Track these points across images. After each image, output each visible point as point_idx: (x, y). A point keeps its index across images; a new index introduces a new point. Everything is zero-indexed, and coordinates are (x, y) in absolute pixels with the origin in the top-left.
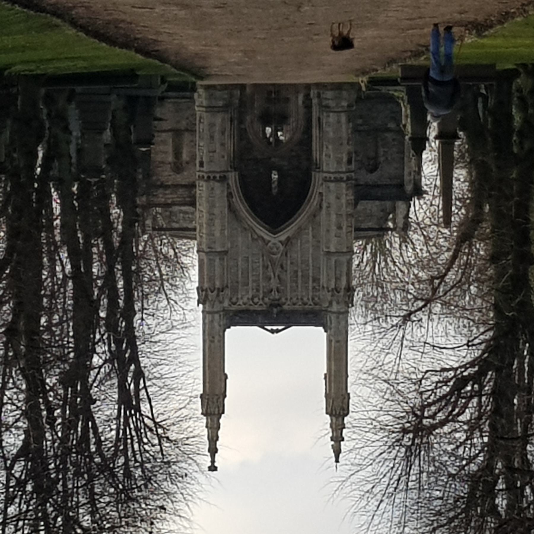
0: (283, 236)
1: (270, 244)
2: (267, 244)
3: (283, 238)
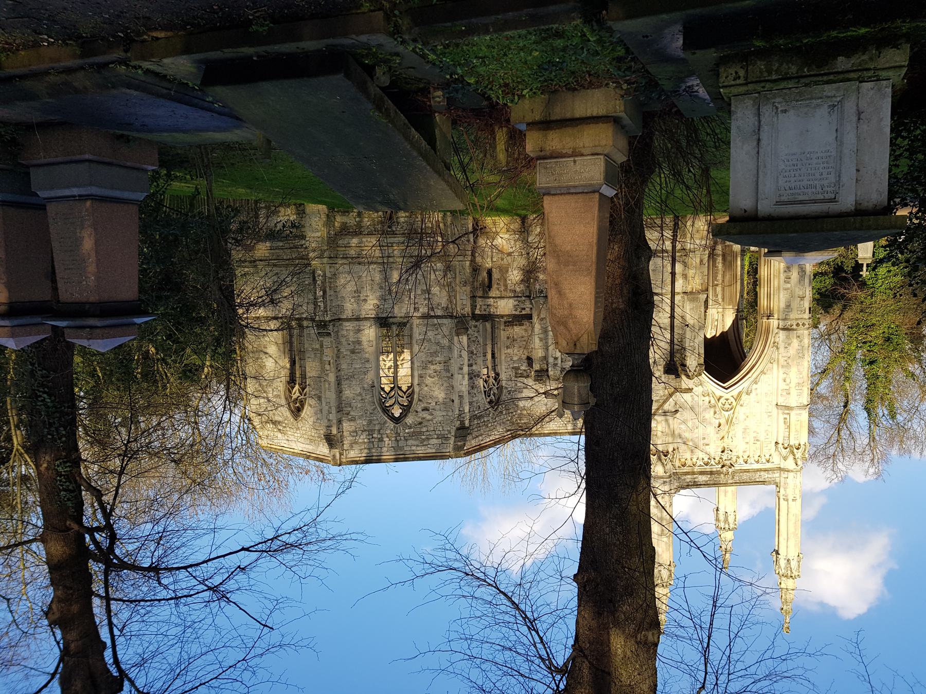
0: (735, 391)
1: (722, 400)
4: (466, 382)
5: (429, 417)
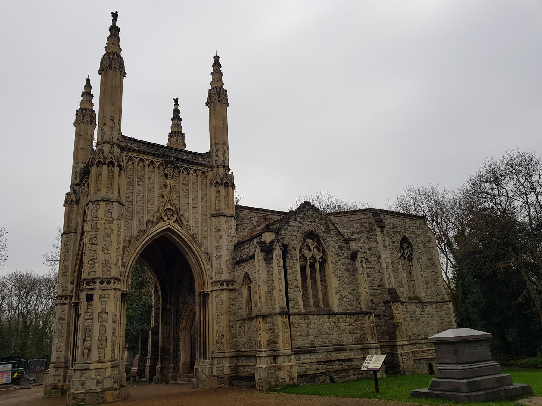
0: (161, 227)
1: (174, 219)
2: (177, 220)
3: (161, 224)
4: (383, 256)
5: (391, 237)
